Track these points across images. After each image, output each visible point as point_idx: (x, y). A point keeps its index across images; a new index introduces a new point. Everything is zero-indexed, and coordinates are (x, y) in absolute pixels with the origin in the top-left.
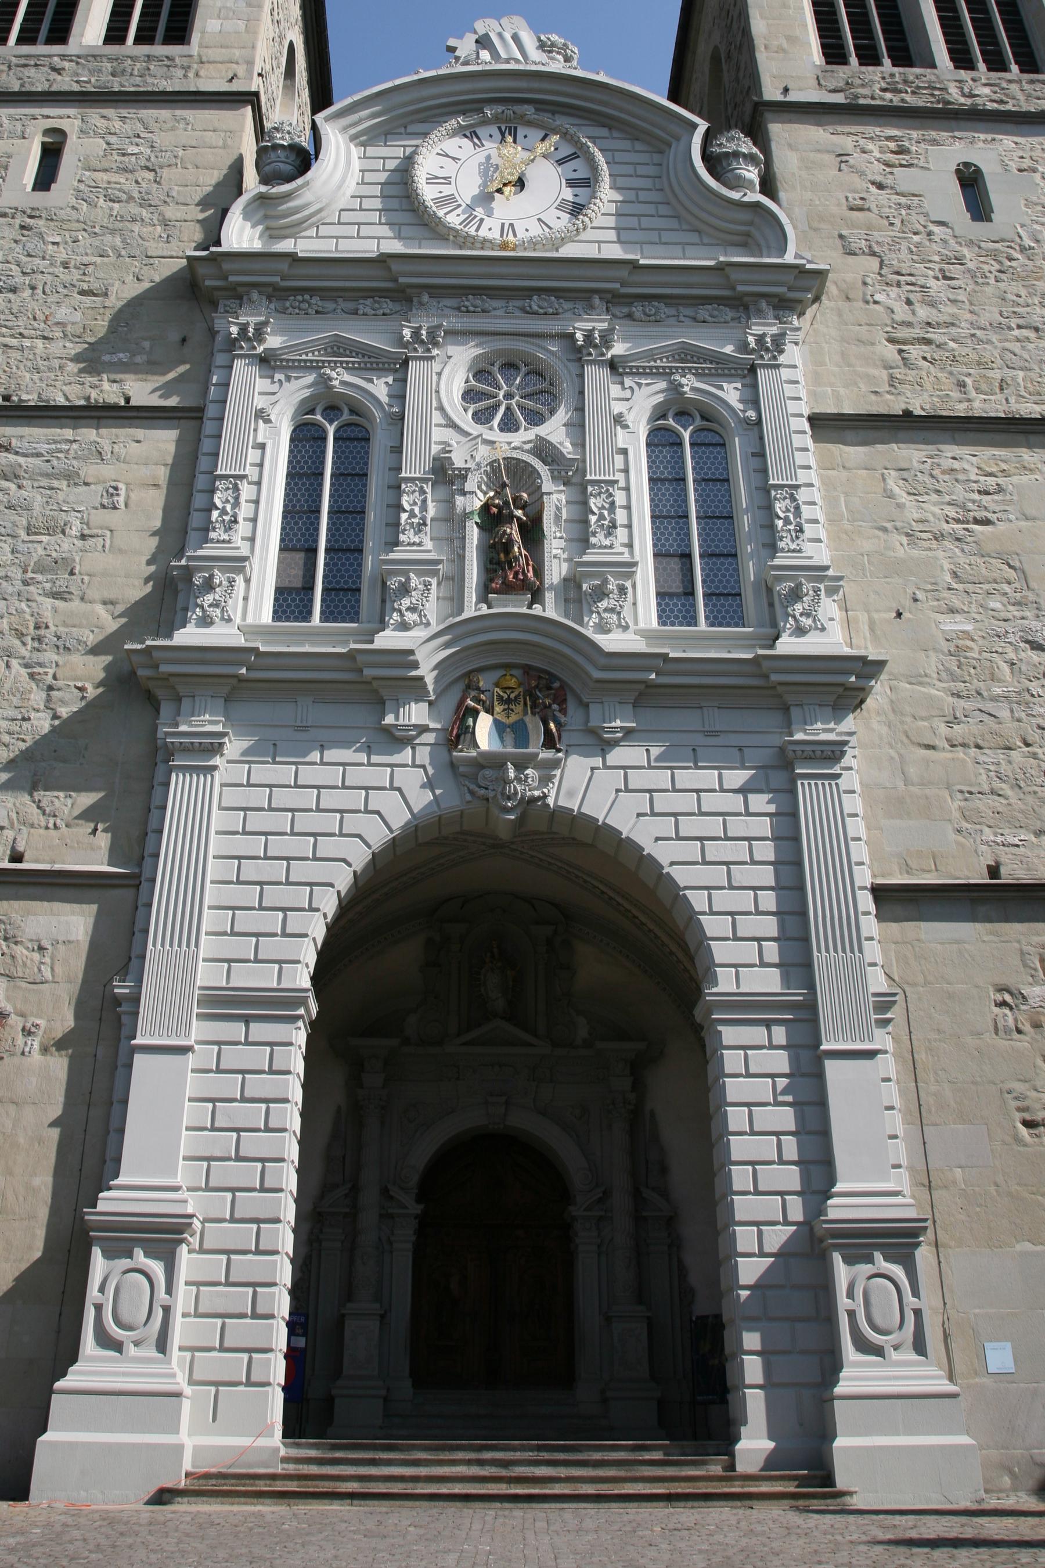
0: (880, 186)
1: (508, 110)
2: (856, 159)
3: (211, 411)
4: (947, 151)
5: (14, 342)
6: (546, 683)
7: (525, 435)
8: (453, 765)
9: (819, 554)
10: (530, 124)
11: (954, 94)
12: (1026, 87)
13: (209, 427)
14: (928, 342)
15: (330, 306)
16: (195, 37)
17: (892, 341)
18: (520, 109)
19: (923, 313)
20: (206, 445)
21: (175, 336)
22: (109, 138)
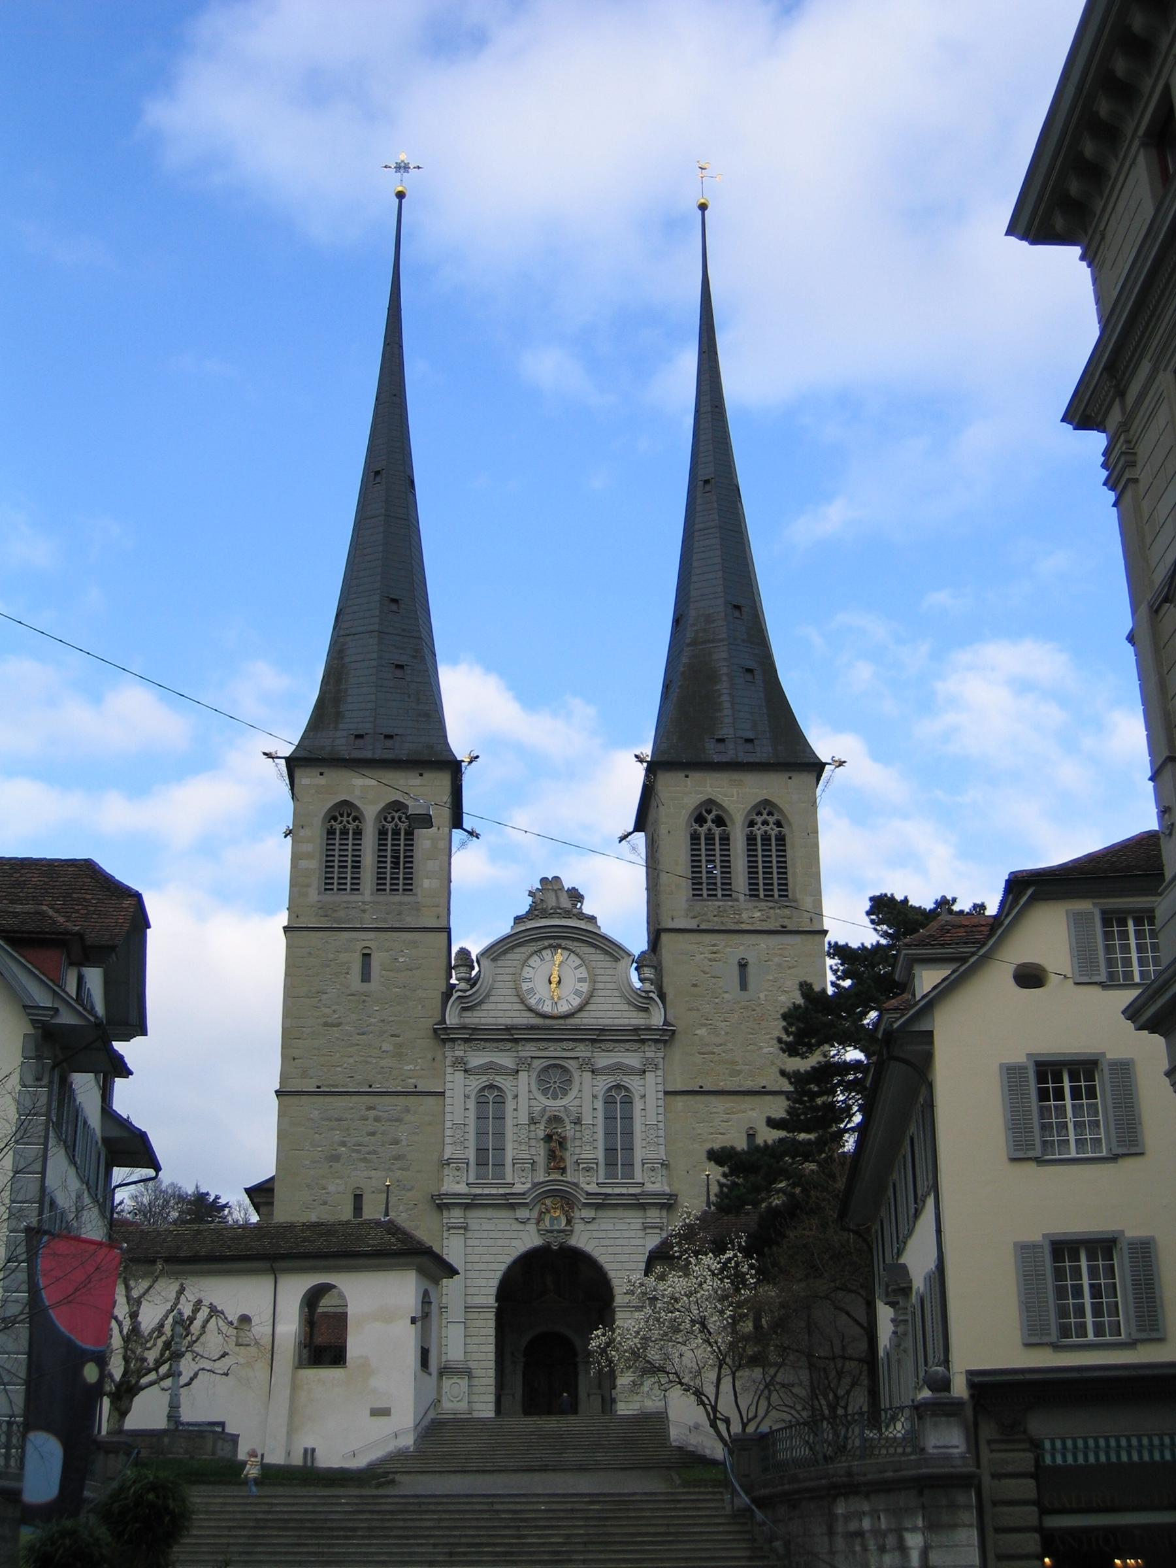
0: (706, 973)
2: (699, 957)
4: (736, 949)
5: (369, 1059)
6: (565, 1199)
7: (559, 1102)
8: (539, 1230)
14: (713, 1053)
15: (488, 1045)
16: (418, 891)
18: (559, 942)
20: (448, 1109)
21: (430, 1057)
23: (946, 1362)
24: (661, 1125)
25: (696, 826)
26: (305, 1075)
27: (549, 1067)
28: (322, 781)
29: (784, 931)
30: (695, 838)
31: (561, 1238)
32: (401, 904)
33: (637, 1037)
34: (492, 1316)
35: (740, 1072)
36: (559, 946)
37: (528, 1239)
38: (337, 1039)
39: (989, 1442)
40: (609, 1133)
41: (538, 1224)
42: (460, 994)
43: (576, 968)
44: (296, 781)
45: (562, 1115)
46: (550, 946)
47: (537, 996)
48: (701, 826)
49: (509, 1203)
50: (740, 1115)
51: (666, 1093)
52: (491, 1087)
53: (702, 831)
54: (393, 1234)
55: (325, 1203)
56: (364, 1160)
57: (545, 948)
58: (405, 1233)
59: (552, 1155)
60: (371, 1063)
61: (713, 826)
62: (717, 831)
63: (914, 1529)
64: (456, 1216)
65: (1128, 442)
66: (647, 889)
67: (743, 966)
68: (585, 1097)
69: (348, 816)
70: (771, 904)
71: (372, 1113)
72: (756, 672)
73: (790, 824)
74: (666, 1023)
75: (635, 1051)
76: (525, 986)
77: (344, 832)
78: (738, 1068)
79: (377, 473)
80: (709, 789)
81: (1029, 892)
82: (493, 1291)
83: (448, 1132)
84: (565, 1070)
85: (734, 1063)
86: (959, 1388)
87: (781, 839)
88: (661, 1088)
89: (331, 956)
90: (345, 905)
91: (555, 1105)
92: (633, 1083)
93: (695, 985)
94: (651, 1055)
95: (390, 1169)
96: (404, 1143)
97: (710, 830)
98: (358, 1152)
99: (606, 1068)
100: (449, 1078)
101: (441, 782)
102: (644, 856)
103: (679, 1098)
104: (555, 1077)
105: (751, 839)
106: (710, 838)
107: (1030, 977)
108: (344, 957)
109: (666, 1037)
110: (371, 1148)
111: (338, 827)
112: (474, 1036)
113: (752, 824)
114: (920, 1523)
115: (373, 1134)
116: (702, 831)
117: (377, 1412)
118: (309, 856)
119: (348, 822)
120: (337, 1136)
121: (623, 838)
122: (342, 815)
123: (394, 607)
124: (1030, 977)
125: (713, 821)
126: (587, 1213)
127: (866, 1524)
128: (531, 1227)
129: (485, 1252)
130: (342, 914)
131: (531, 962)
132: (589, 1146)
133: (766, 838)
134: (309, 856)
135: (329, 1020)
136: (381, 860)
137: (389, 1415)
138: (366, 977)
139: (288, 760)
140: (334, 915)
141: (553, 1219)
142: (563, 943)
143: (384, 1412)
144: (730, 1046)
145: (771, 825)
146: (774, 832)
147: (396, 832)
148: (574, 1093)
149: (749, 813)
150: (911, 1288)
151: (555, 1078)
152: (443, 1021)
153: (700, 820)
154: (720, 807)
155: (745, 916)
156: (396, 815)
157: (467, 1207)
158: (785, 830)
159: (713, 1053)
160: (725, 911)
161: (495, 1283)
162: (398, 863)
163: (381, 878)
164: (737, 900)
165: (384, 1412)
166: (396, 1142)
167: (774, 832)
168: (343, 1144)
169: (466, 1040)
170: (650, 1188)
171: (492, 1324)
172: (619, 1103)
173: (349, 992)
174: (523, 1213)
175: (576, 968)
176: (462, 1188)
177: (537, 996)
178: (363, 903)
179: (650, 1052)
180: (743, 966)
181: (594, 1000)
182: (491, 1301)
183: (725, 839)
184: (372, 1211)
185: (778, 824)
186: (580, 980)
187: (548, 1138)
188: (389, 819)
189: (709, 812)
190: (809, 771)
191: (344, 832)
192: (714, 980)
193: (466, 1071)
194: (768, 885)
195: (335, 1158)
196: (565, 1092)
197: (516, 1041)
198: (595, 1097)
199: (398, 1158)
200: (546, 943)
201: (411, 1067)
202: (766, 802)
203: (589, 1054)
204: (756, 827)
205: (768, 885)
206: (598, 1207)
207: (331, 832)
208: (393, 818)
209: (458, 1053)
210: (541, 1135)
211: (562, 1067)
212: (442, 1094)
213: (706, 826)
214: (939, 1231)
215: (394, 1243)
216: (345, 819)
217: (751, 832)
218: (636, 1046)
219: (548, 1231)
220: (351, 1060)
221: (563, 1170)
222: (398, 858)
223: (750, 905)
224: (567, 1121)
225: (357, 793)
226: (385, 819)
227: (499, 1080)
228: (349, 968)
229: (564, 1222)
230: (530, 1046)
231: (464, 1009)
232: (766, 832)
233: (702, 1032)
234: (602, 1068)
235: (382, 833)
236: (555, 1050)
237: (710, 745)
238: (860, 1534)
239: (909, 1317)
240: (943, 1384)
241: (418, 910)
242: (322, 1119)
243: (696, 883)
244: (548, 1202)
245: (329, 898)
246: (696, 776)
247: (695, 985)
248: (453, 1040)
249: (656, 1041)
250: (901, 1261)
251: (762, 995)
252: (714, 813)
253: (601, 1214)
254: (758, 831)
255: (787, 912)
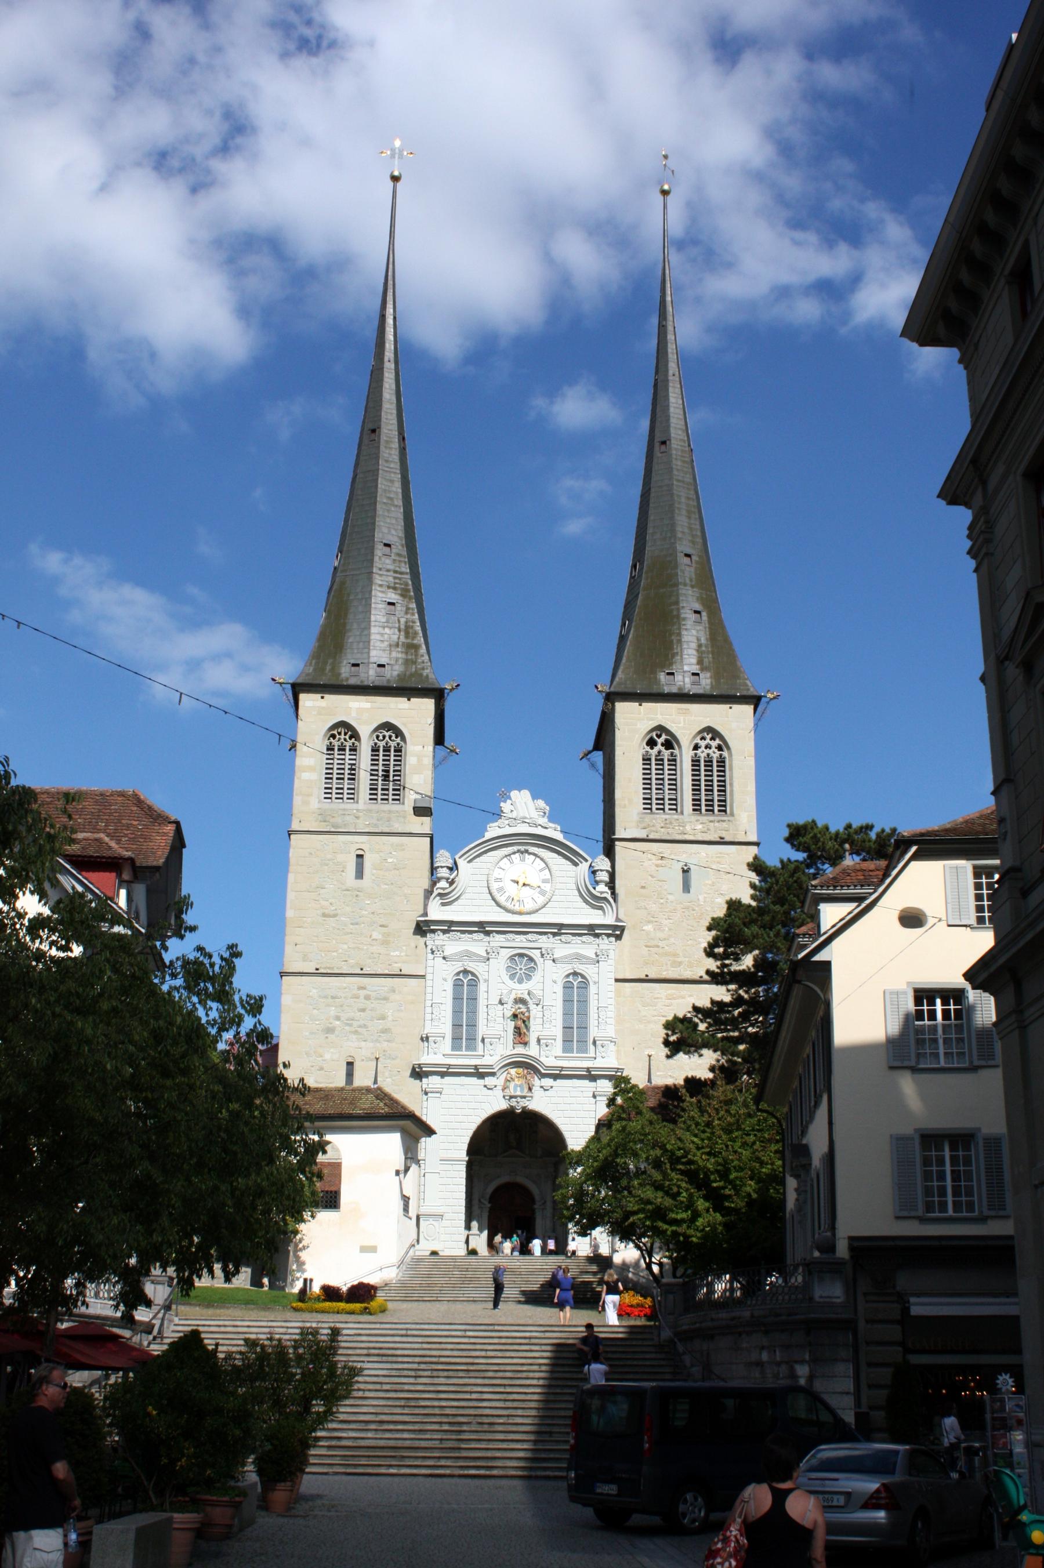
0: (652, 876)
1: (522, 848)
3: (429, 977)
5: (361, 946)
9: (610, 1031)
10: (530, 854)
11: (688, 828)
12: (717, 824)
13: (429, 983)
14: (658, 947)
17: (646, 946)
18: (526, 848)
19: (660, 935)
20: (429, 990)
21: (413, 945)
22: (382, 854)
23: (833, 1228)
24: (611, 1008)
25: (648, 748)
26: (305, 958)
27: (515, 955)
28: (323, 703)
29: (722, 842)
30: (646, 760)
31: (524, 1103)
32: (390, 812)
33: (592, 930)
34: (463, 1168)
35: (680, 963)
36: (527, 851)
37: (497, 1104)
38: (334, 928)
39: (865, 1294)
40: (567, 1014)
41: (503, 1090)
42: (442, 891)
43: (541, 870)
44: (301, 703)
45: (527, 997)
46: (518, 851)
47: (507, 895)
48: (652, 748)
49: (479, 1074)
50: (680, 1001)
51: (617, 980)
52: (466, 972)
53: (654, 752)
54: (381, 1100)
55: (321, 1069)
56: (356, 1032)
57: (514, 853)
58: (392, 1099)
59: (518, 1031)
60: (362, 949)
61: (663, 749)
62: (666, 753)
63: (802, 1362)
64: (433, 1082)
65: (986, 522)
66: (604, 801)
67: (686, 871)
68: (547, 985)
69: (345, 734)
70: (712, 818)
71: (362, 993)
72: (704, 614)
73: (728, 748)
74: (618, 919)
75: (590, 943)
76: (494, 886)
77: (342, 749)
78: (679, 960)
79: (374, 431)
80: (659, 716)
81: (914, 849)
82: (465, 1147)
83: (429, 1010)
84: (531, 959)
85: (676, 955)
86: (842, 1250)
87: (722, 762)
88: (613, 976)
89: (329, 856)
90: (341, 812)
91: (522, 990)
92: (589, 971)
93: (643, 887)
94: (605, 947)
95: (377, 1041)
96: (390, 1018)
97: (659, 752)
98: (351, 1025)
99: (566, 957)
100: (430, 963)
101: (427, 706)
102: (601, 771)
103: (627, 984)
104: (522, 965)
105: (696, 762)
106: (660, 761)
107: (912, 919)
108: (340, 858)
109: (617, 932)
110: (362, 1022)
111: (336, 743)
112: (449, 927)
113: (696, 747)
114: (807, 1357)
115: (363, 1010)
116: (654, 752)
117: (364, 1249)
118: (311, 769)
119: (345, 740)
120: (333, 1011)
121: (586, 755)
122: (340, 734)
123: (388, 549)
124: (912, 919)
125: (662, 745)
126: (548, 1082)
127: (765, 1356)
128: (498, 1093)
129: (457, 1114)
130: (339, 820)
131: (502, 864)
132: (548, 1022)
133: (709, 762)
134: (311, 769)
135: (326, 911)
136: (373, 773)
137: (375, 1252)
138: (360, 874)
139: (294, 686)
140: (332, 820)
141: (516, 1086)
142: (532, 849)
143: (373, 1249)
144: (672, 940)
145: (713, 749)
146: (715, 755)
147: (387, 749)
148: (537, 977)
149: (695, 737)
150: (810, 1164)
151: (523, 964)
152: (425, 914)
153: (652, 743)
154: (668, 732)
155: (688, 828)
156: (387, 734)
157: (443, 1075)
158: (725, 754)
159: (658, 947)
160: (671, 823)
161: (467, 1140)
162: (388, 776)
163: (373, 789)
164: (682, 813)
165: (373, 1249)
166: (383, 1018)
167: (715, 755)
168: (338, 1018)
169: (444, 932)
170: (599, 1063)
171: (464, 1174)
172: (576, 989)
173: (344, 888)
174: (489, 1081)
175: (541, 870)
176: (439, 1059)
177: (507, 895)
178: (358, 810)
179: (606, 944)
180: (686, 871)
181: (554, 898)
182: (463, 1155)
183: (673, 761)
184: (363, 1079)
185: (719, 748)
186: (544, 881)
187: (515, 1016)
188: (381, 738)
189: (659, 736)
190: (747, 703)
191: (342, 749)
192: (660, 883)
193: (444, 958)
194: (710, 802)
195: (330, 1030)
196: (529, 977)
197: (488, 933)
198: (555, 982)
199: (385, 1031)
200: (515, 848)
201: (397, 953)
202: (709, 730)
203: (550, 946)
204: (700, 750)
205: (710, 802)
206: (555, 1077)
207: (330, 748)
208: (384, 737)
209: (437, 943)
210: (509, 1014)
211: (527, 956)
212: (423, 977)
213: (656, 749)
214: (830, 1123)
215: (383, 1108)
216: (342, 737)
217: (696, 755)
218: (592, 938)
219: (511, 1097)
220: (345, 946)
221: (525, 1044)
222: (388, 771)
223: (694, 818)
224: (530, 1002)
225: (354, 714)
226: (378, 737)
227: (471, 966)
228: (345, 867)
229: (526, 1090)
230: (498, 937)
231: (443, 904)
232: (708, 755)
233: (649, 928)
234: (561, 958)
235: (375, 750)
236: (521, 941)
237: (662, 677)
238: (759, 1364)
239: (808, 1188)
240: (829, 1247)
241: (404, 817)
242: (320, 997)
243: (647, 800)
244: (513, 1071)
245: (327, 805)
246: (647, 706)
247: (643, 887)
248: (434, 931)
249: (608, 935)
250: (804, 1142)
251: (701, 898)
252: (664, 737)
253: (560, 1082)
254: (702, 753)
255: (725, 825)
